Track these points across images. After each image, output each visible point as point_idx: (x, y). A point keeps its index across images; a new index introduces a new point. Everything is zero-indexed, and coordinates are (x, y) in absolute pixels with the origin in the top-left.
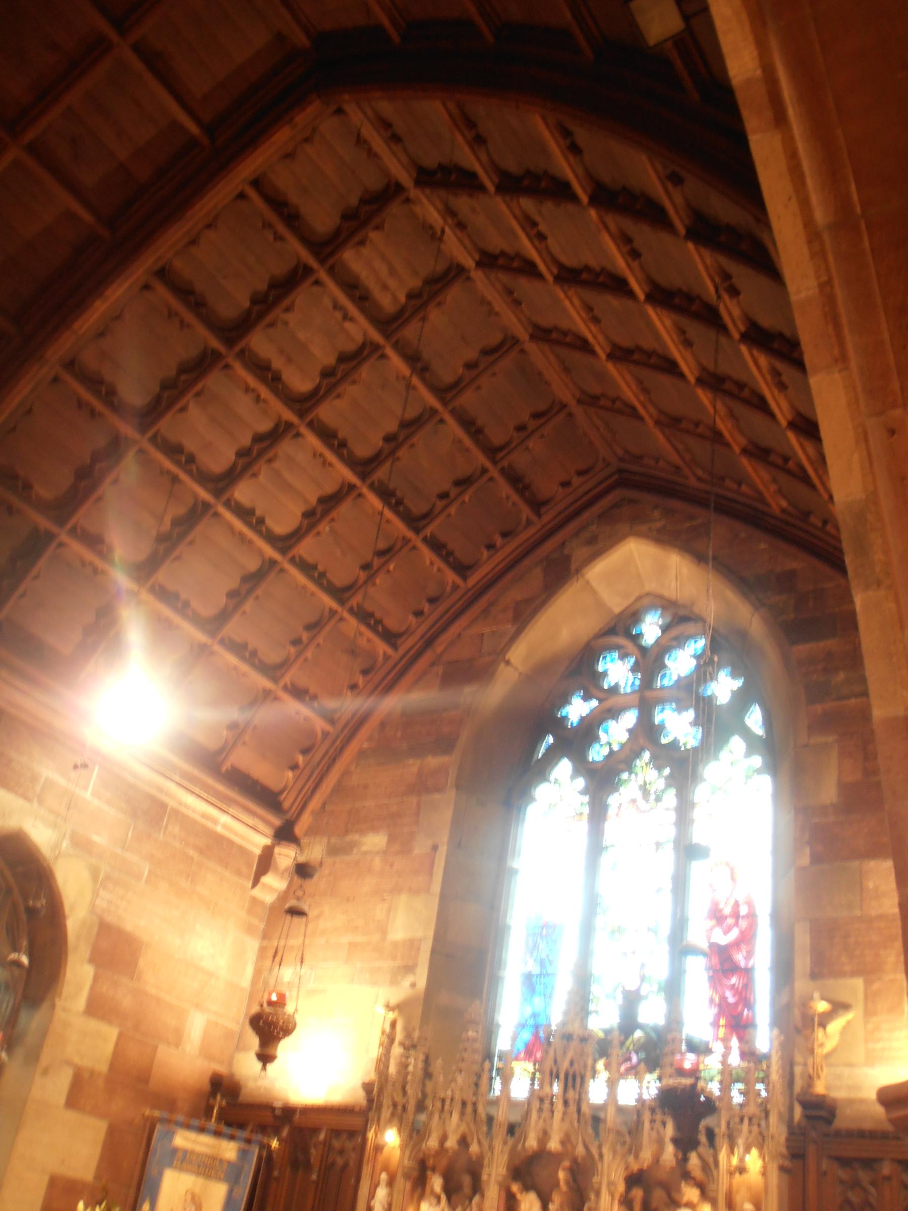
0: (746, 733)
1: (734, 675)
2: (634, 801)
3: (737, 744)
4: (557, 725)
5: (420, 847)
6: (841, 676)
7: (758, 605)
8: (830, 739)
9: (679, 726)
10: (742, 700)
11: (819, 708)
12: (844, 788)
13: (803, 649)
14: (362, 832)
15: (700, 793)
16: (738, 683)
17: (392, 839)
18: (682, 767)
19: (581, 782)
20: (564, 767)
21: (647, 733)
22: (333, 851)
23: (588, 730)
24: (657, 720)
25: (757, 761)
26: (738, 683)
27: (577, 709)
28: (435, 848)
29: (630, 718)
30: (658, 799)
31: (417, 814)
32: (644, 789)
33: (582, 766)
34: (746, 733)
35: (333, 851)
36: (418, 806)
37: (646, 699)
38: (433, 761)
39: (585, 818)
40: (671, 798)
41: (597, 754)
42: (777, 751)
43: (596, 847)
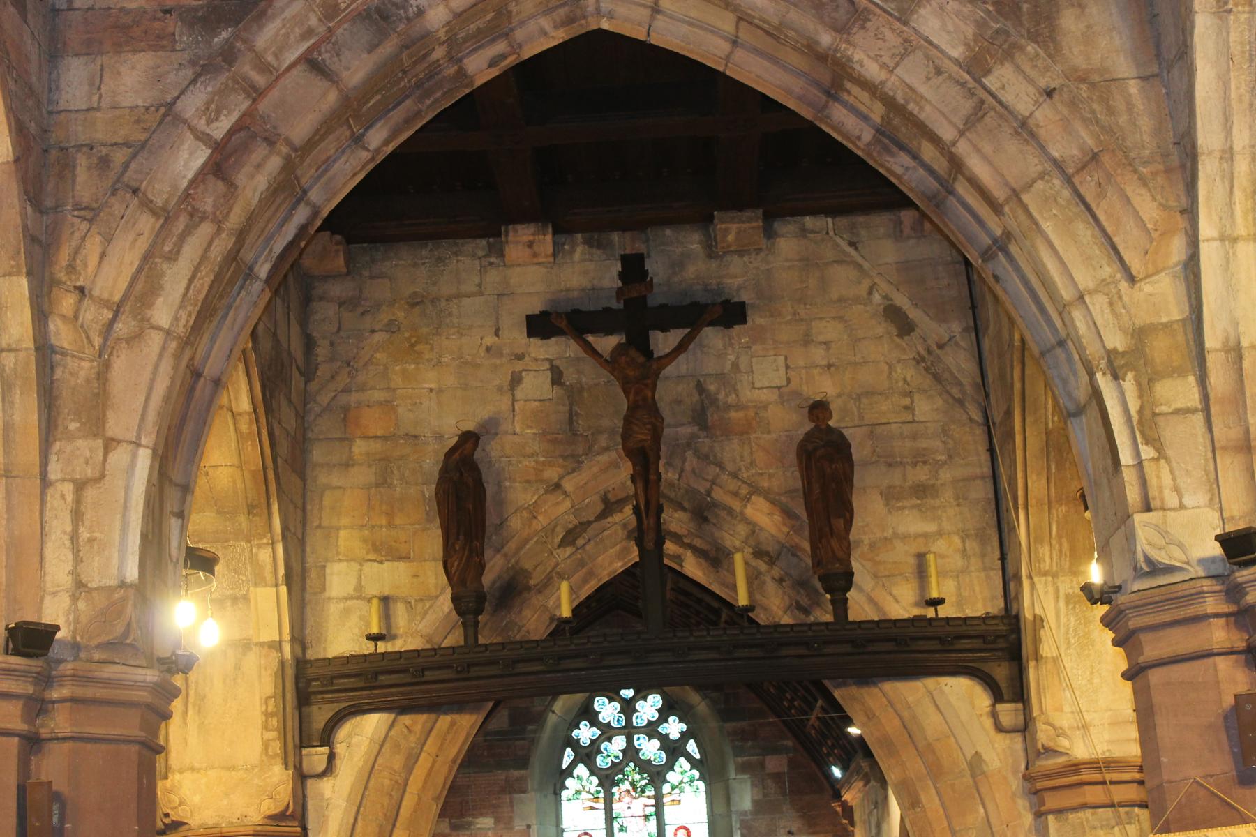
0: (689, 757)
1: (681, 721)
2: (628, 791)
3: (682, 763)
4: (574, 744)
5: (519, 825)
6: (750, 743)
7: (705, 697)
8: (746, 776)
9: (650, 749)
10: (685, 736)
11: (740, 760)
12: (755, 803)
13: (729, 726)
14: (475, 817)
15: (666, 788)
16: (683, 727)
17: (497, 820)
18: (656, 775)
19: (595, 780)
20: (581, 770)
21: (631, 752)
22: (454, 827)
23: (595, 745)
24: (636, 743)
25: (696, 774)
26: (683, 727)
27: (585, 733)
28: (529, 826)
29: (619, 742)
30: (643, 791)
31: (512, 806)
32: (633, 784)
33: (593, 771)
34: (689, 757)
35: (454, 827)
36: (511, 802)
37: (629, 730)
38: (516, 773)
39: (602, 800)
40: (650, 792)
41: (601, 762)
42: (709, 769)
43: (610, 818)
